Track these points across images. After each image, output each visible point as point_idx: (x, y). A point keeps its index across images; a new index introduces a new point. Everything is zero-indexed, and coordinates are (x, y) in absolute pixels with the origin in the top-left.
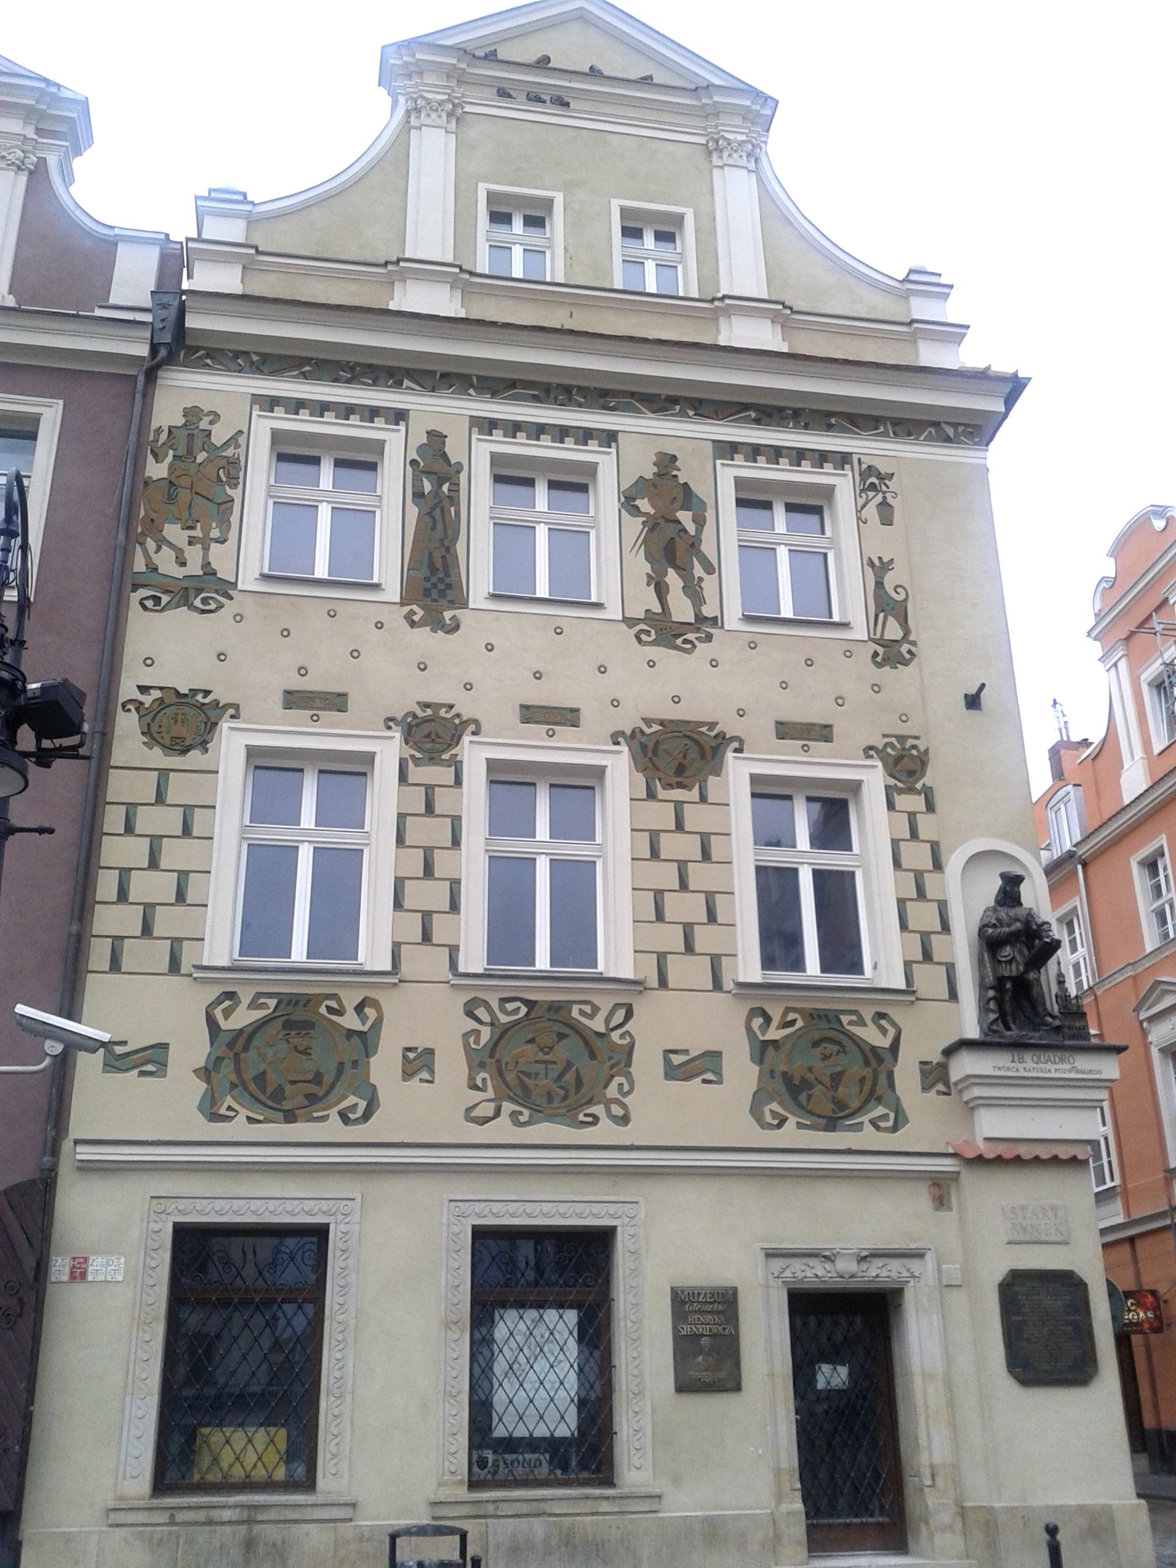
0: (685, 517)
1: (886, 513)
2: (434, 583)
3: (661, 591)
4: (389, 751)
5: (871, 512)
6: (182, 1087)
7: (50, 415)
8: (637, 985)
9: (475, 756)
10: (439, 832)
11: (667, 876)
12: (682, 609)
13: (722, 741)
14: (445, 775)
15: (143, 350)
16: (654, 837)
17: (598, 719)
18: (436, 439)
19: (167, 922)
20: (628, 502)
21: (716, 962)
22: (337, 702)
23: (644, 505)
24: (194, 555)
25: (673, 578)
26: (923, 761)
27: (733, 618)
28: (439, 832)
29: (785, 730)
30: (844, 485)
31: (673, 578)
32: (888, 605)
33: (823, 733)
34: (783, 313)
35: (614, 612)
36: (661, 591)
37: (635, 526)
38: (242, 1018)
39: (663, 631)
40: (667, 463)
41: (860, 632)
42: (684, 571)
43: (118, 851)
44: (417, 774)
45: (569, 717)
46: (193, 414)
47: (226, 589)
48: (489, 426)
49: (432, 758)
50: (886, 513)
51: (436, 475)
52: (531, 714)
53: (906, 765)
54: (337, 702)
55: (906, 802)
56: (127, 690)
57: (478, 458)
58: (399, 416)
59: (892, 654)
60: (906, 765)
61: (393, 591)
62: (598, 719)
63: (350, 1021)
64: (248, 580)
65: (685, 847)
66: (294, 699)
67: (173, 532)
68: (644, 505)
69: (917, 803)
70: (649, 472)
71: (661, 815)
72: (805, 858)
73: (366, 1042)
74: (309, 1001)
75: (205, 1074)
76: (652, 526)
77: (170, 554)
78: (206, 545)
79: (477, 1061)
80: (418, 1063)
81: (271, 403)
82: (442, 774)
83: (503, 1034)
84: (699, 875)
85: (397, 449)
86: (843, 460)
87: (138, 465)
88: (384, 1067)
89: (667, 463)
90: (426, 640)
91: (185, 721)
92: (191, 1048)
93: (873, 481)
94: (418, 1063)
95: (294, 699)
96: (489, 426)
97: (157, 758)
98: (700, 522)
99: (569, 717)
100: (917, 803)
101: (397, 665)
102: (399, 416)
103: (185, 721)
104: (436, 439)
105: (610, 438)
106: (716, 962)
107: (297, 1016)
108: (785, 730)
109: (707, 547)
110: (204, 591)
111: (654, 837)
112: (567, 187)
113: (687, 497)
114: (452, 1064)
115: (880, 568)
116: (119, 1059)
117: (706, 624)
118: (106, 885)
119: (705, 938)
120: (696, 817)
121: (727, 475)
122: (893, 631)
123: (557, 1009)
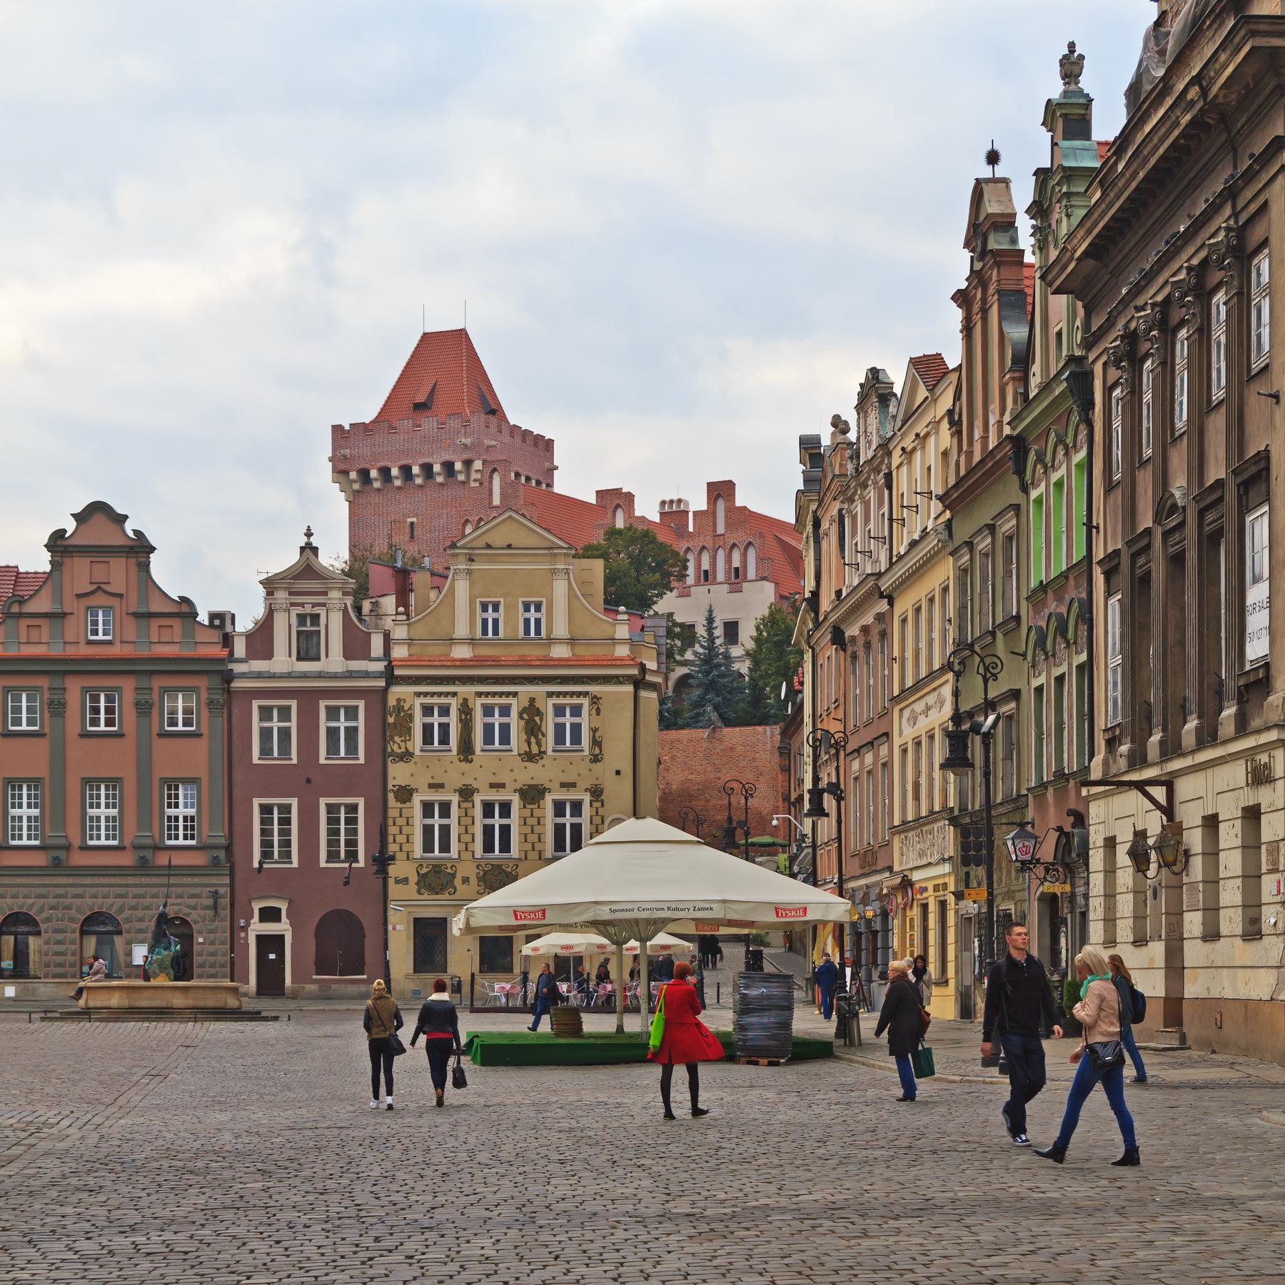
0: (537, 719)
1: (598, 712)
2: (466, 749)
3: (529, 744)
4: (455, 799)
5: (594, 711)
6: (412, 887)
7: (361, 704)
8: (519, 859)
9: (478, 799)
10: (469, 821)
11: (528, 829)
12: (535, 750)
13: (545, 789)
14: (470, 805)
15: (383, 684)
16: (525, 819)
17: (511, 786)
18: (465, 700)
19: (406, 847)
20: (520, 717)
21: (540, 852)
22: (441, 786)
23: (525, 716)
24: (403, 745)
25: (533, 740)
26: (602, 792)
27: (550, 752)
28: (469, 821)
29: (563, 785)
30: (585, 702)
31: (533, 740)
32: (596, 743)
33: (573, 785)
34: (572, 641)
35: (515, 753)
36: (529, 744)
37: (522, 723)
38: (424, 870)
39: (529, 757)
40: (532, 700)
41: (587, 753)
42: (536, 737)
43: (392, 830)
44: (463, 805)
45: (503, 786)
46: (399, 700)
47: (412, 755)
48: (479, 694)
49: (466, 801)
50: (598, 712)
51: (466, 710)
52: (492, 786)
53: (596, 793)
54: (441, 786)
55: (595, 804)
56: (390, 787)
57: (477, 705)
58: (454, 694)
59: (596, 759)
60: (596, 793)
61: (455, 752)
62: (511, 786)
63: (449, 871)
64: (417, 752)
65: (532, 821)
66: (431, 786)
67: (397, 739)
68: (525, 716)
69: (599, 804)
70: (527, 704)
71: (527, 813)
72: (568, 820)
73: (454, 875)
74: (440, 866)
75: (417, 884)
76: (527, 722)
77: (396, 746)
78: (405, 741)
79: (479, 880)
80: (466, 880)
81: (418, 694)
82: (469, 805)
83: (486, 873)
84: (537, 829)
85: (454, 704)
86: (586, 694)
87: (385, 719)
88: (458, 882)
89: (532, 700)
90: (464, 765)
91: (405, 794)
92: (414, 878)
93: (595, 700)
94: (466, 880)
95: (431, 786)
96: (479, 694)
97: (399, 805)
98: (541, 720)
99: (503, 786)
100: (599, 804)
101: (456, 773)
102: (454, 694)
103: (405, 794)
104: (465, 700)
105: (515, 694)
106: (540, 852)
107: (437, 869)
108: (563, 785)
109: (543, 729)
110: (406, 756)
111: (525, 819)
112: (505, 595)
113: (538, 712)
114: (473, 880)
115: (594, 731)
116: (397, 881)
117: (542, 753)
118: (391, 839)
119: (538, 846)
120: (537, 813)
121: (552, 701)
122: (597, 751)
123: (499, 866)
